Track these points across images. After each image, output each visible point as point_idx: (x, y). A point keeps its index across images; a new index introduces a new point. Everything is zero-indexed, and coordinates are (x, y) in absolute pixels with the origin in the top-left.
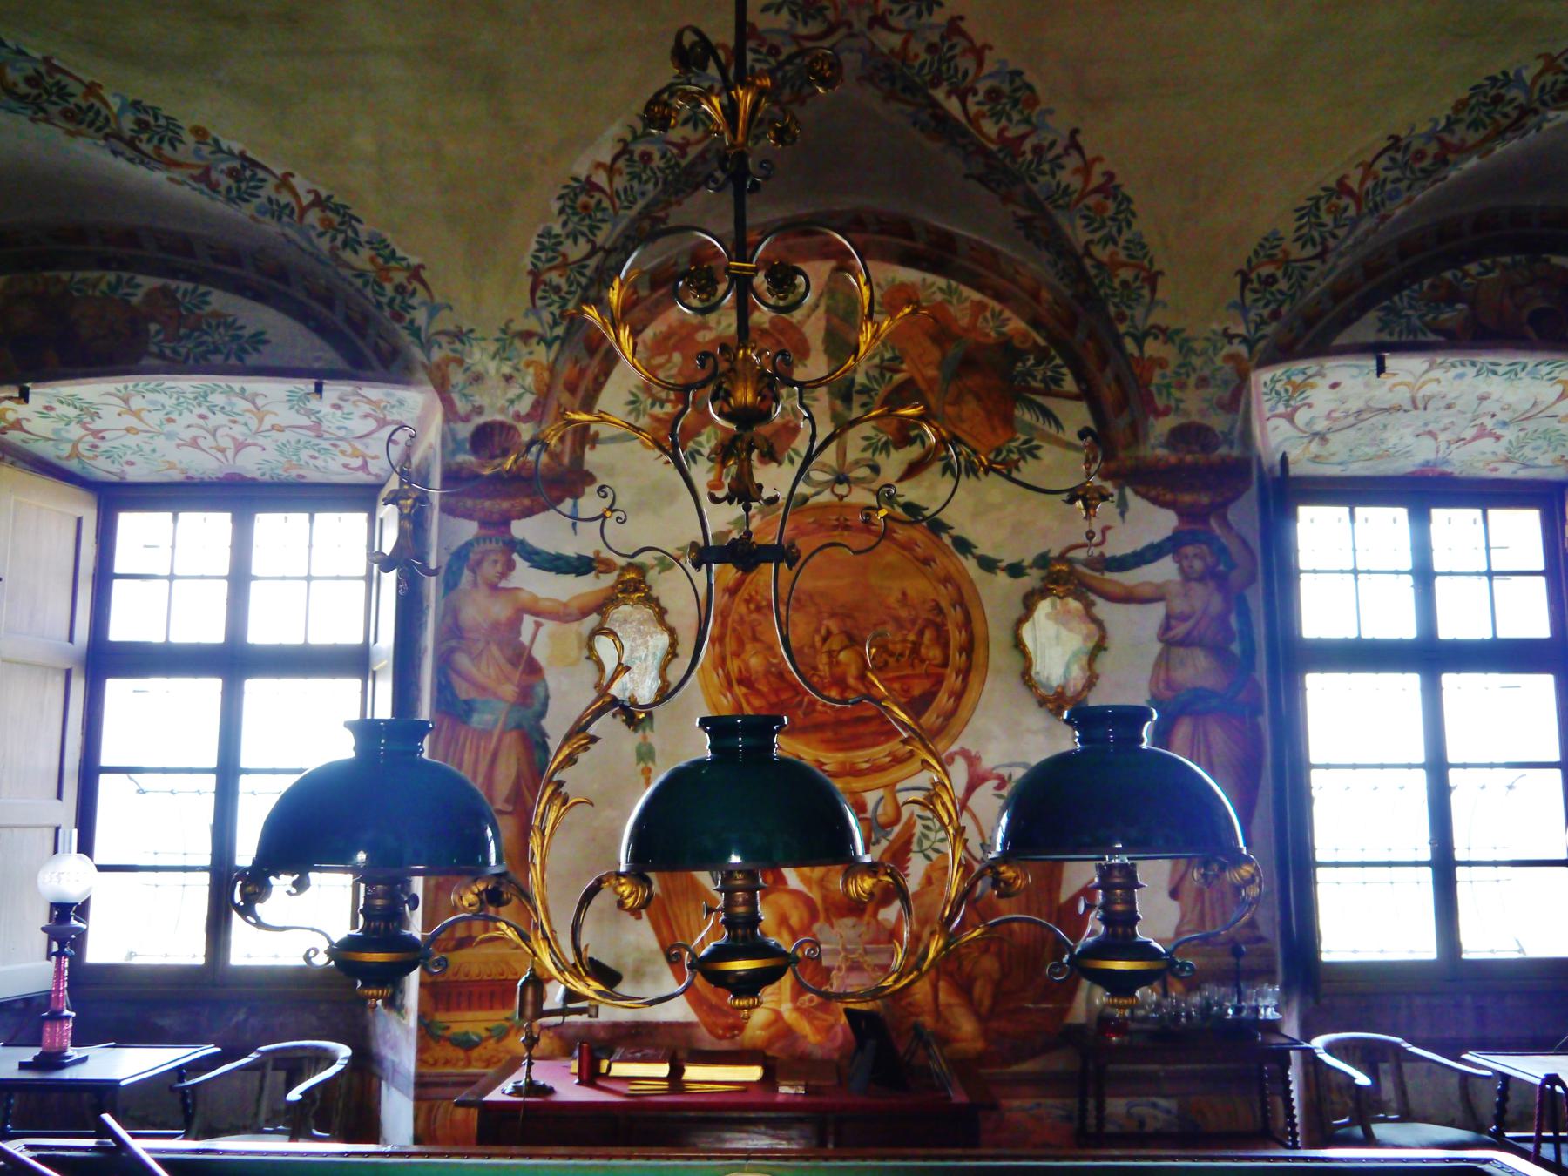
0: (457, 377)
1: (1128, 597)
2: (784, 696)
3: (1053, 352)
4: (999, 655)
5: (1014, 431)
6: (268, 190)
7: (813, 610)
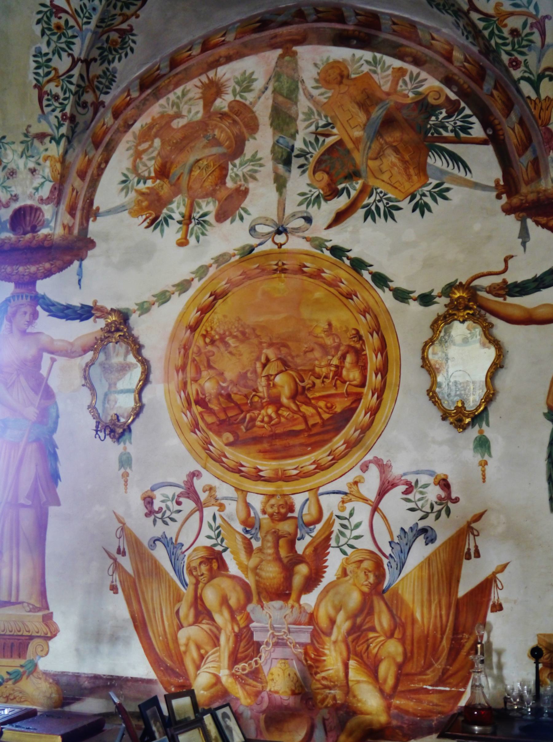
1: (529, 319)
2: (230, 414)
4: (410, 376)
5: (427, 177)
7: (255, 341)
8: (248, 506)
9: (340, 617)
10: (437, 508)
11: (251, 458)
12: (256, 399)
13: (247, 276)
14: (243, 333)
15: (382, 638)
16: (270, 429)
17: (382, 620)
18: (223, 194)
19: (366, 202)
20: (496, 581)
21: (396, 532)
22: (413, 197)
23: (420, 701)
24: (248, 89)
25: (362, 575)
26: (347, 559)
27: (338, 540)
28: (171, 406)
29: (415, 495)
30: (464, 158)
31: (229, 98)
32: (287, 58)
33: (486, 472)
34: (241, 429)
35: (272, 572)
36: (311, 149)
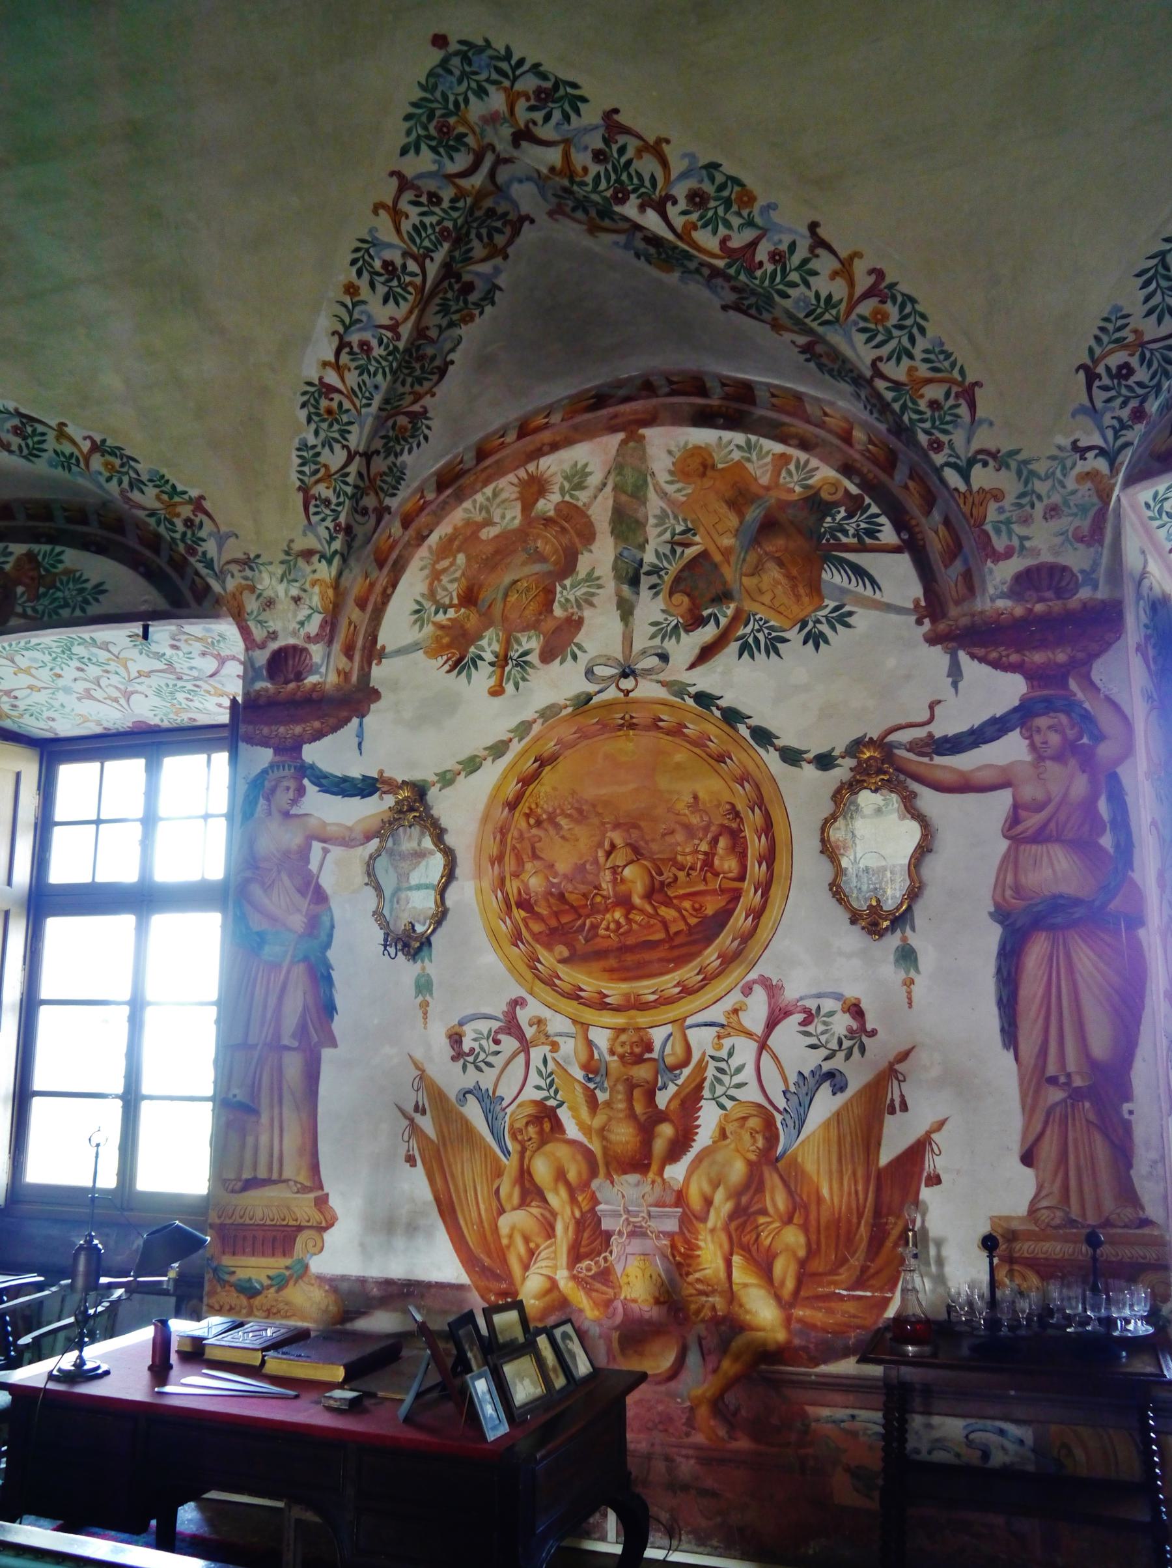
0: (251, 604)
1: (964, 786)
2: (564, 920)
3: (867, 500)
4: (806, 866)
6: (51, 443)
7: (595, 821)
8: (590, 1044)
9: (719, 1196)
10: (847, 1044)
12: (598, 899)
13: (583, 735)
14: (580, 811)
15: (777, 1224)
17: (777, 1199)
18: (549, 625)
19: (740, 632)
20: (930, 1144)
21: (792, 1078)
22: (804, 624)
23: (831, 1311)
24: (580, 486)
25: (747, 1137)
26: (726, 1115)
27: (713, 1089)
28: (484, 910)
29: (816, 1027)
30: (872, 572)
31: (556, 498)
32: (632, 444)
33: (913, 994)
35: (624, 1135)
36: (666, 564)
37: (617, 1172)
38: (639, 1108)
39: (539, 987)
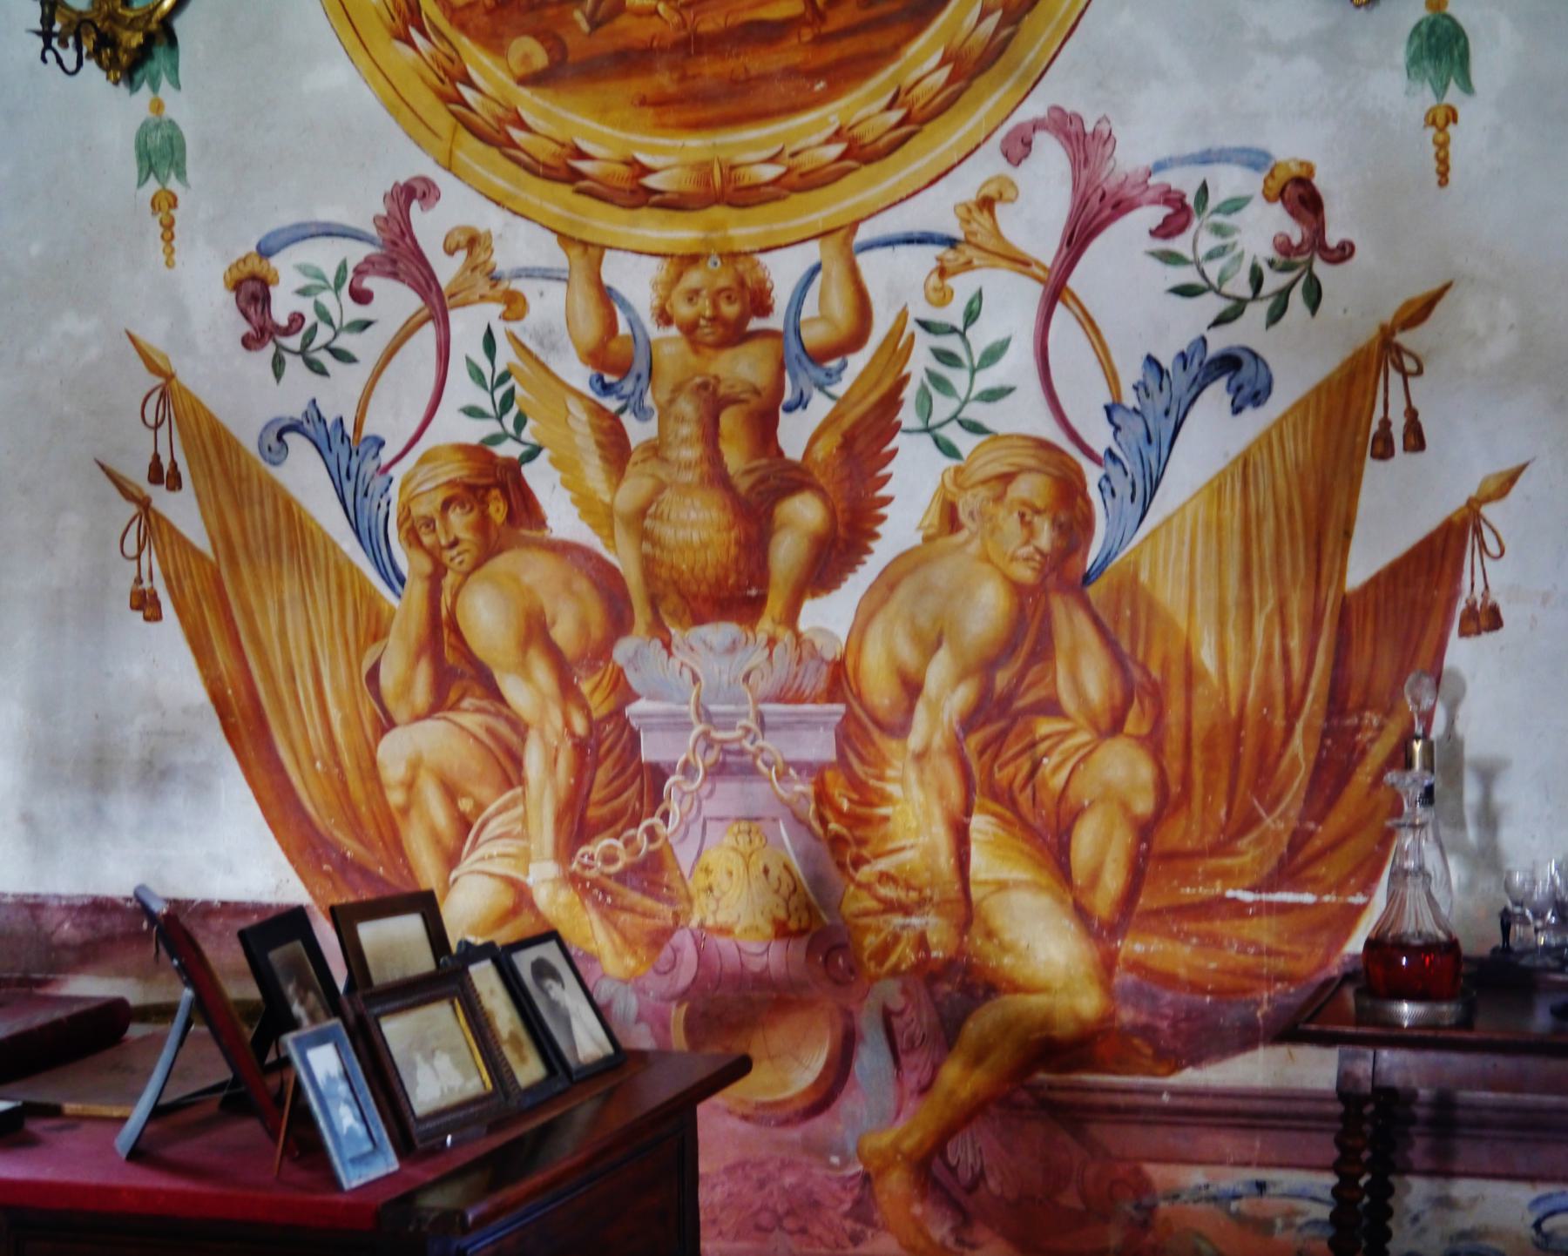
8: (606, 297)
9: (938, 672)
10: (1273, 281)
11: (613, 125)
15: (1083, 737)
16: (676, 19)
17: (1084, 674)
20: (1478, 531)
21: (1131, 372)
23: (1212, 942)
25: (1010, 524)
26: (958, 471)
27: (925, 405)
29: (1196, 240)
33: (1451, 149)
34: (574, 23)
35: (698, 528)
37: (680, 623)
38: (735, 458)
39: (470, 149)
